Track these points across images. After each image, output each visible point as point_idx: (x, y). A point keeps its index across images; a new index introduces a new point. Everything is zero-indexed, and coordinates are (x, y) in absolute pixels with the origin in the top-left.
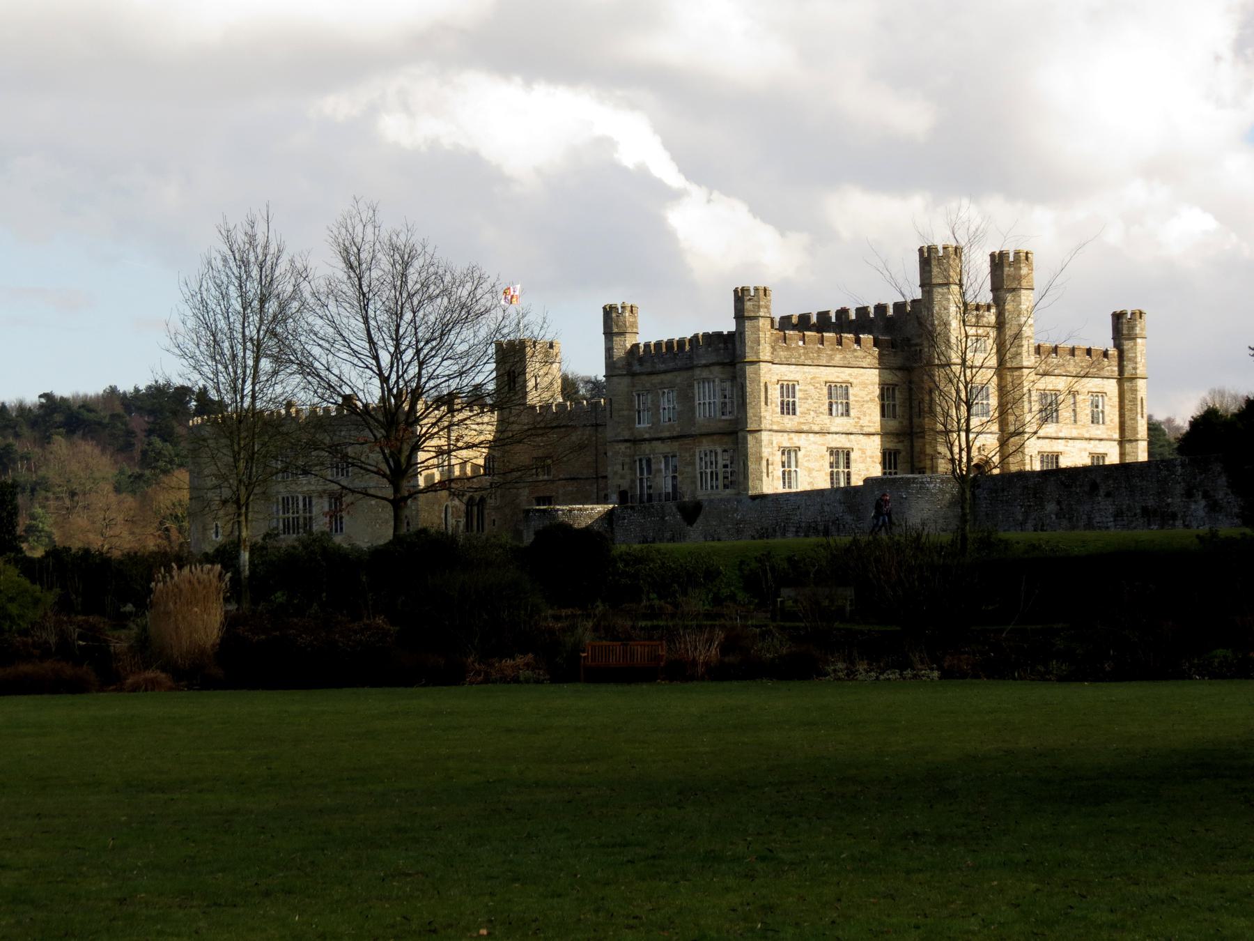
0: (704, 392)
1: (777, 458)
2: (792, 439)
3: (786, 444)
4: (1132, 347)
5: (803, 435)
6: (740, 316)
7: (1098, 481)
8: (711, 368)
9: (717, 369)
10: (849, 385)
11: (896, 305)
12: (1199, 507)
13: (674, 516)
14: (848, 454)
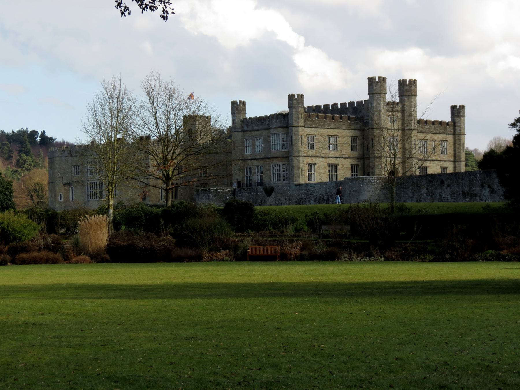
0: (275, 139)
1: (306, 168)
2: (312, 160)
4: (459, 121)
5: (317, 158)
6: (290, 107)
7: (444, 180)
8: (278, 129)
9: (280, 130)
10: (337, 137)
11: (358, 102)
12: (486, 191)
13: (262, 193)
14: (336, 167)
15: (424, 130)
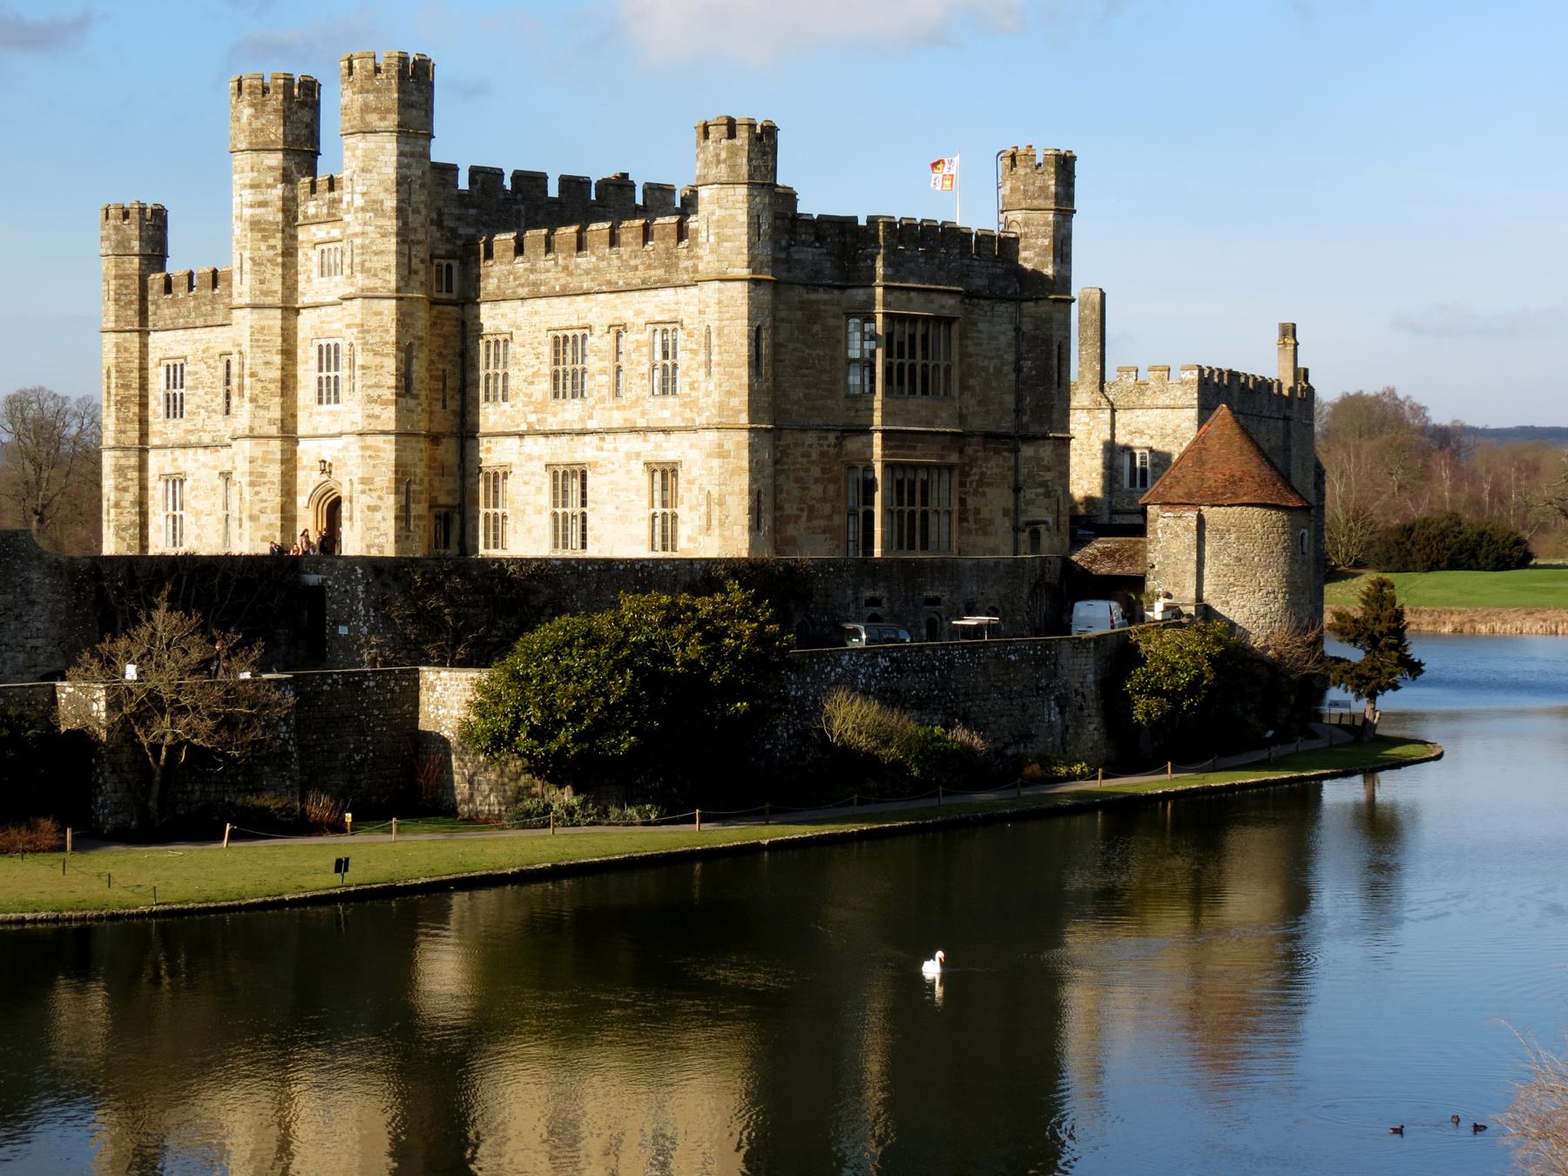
3: (169, 470)
5: (190, 452)
15: (574, 283)
